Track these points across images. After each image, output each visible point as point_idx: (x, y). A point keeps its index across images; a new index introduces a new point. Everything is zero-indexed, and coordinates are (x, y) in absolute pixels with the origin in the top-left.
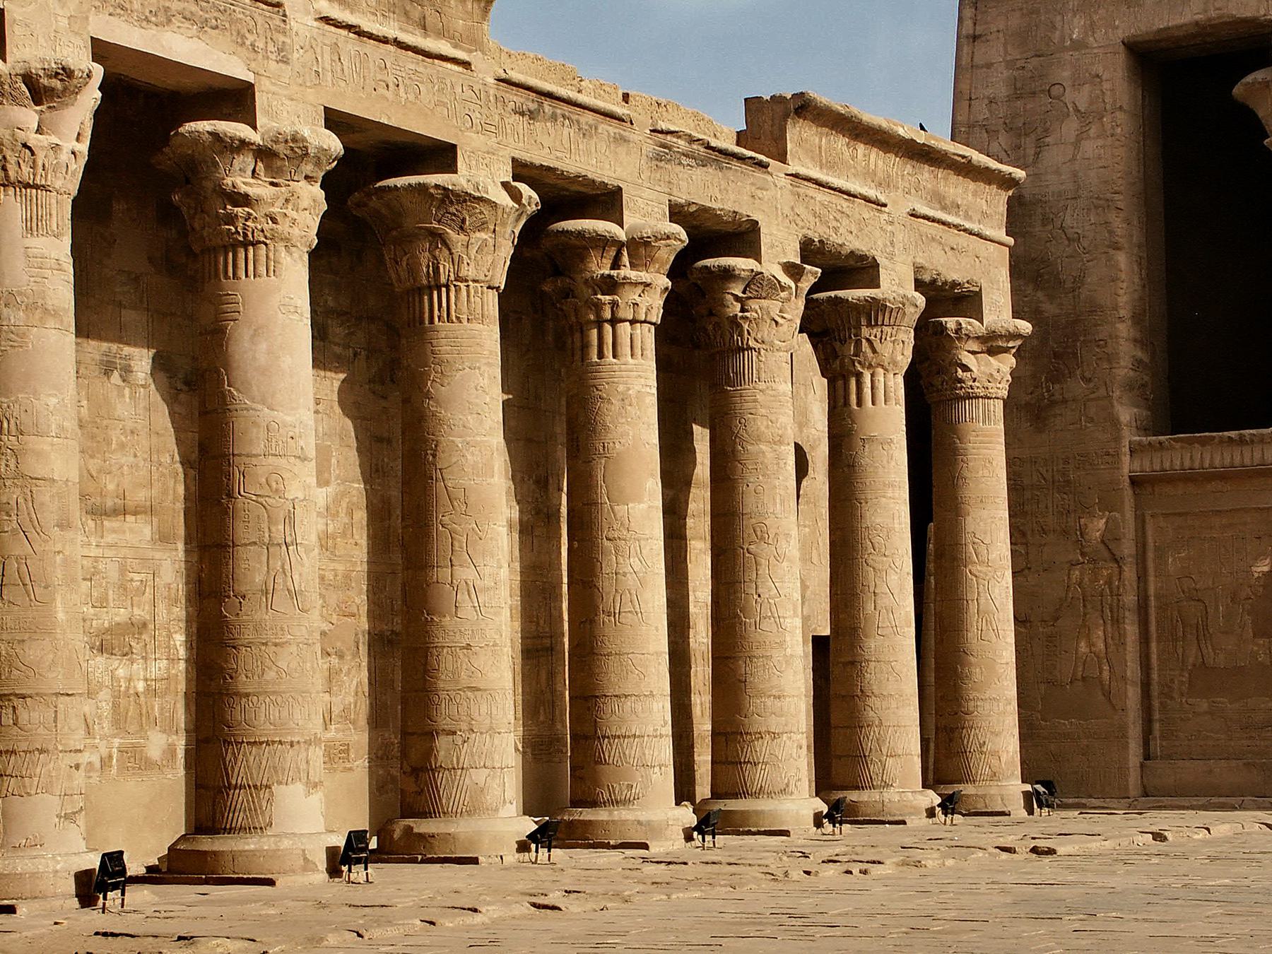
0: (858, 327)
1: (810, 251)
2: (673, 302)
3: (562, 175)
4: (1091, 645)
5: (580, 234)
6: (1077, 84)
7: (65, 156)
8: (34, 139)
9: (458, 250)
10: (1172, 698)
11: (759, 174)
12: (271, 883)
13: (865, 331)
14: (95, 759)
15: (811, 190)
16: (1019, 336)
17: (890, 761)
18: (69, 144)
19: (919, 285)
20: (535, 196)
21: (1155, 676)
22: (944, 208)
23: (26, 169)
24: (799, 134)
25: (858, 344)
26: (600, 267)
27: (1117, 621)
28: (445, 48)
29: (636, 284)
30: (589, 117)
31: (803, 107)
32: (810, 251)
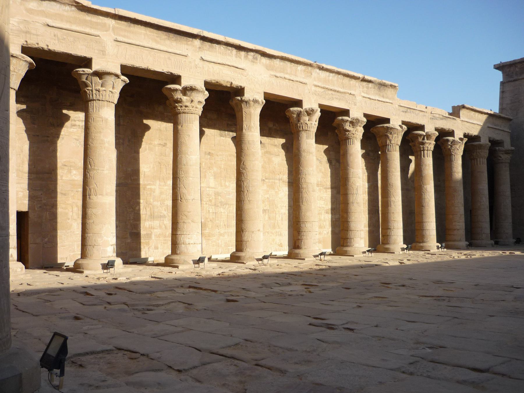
1: (465, 136)
2: (436, 146)
3: (412, 123)
5: (416, 134)
7: (313, 125)
8: (308, 122)
9: (391, 138)
11: (454, 121)
12: (353, 256)
14: (326, 232)
15: (466, 123)
18: (314, 123)
19: (490, 141)
20: (406, 127)
23: (306, 128)
24: (463, 112)
26: (420, 140)
28: (387, 100)
30: (417, 112)
31: (463, 107)
32: (465, 136)
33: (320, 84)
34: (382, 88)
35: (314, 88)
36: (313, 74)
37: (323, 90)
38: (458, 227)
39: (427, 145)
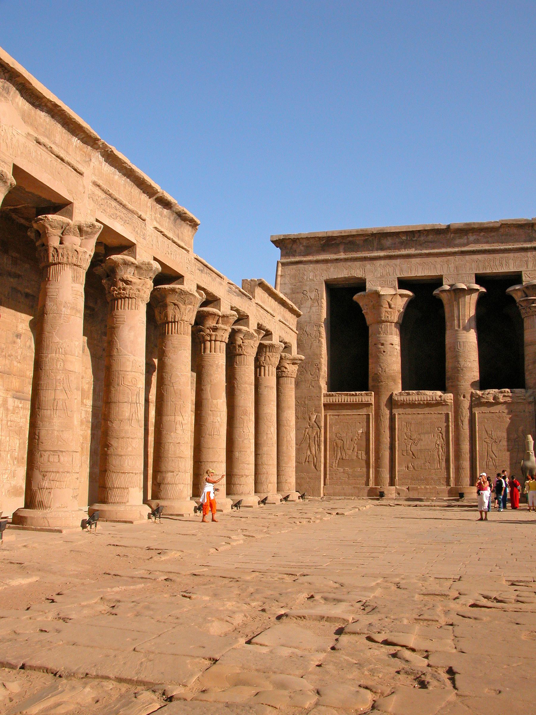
0: (265, 352)
4: (311, 451)
6: (311, 291)
8: (79, 249)
9: (182, 310)
10: (332, 467)
13: (268, 354)
15: (259, 308)
16: (301, 360)
17: (270, 485)
21: (328, 461)
22: (285, 320)
25: (265, 357)
27: (319, 446)
29: (223, 329)
30: (214, 275)
33: (100, 182)
34: (179, 221)
35: (91, 187)
36: (93, 160)
37: (104, 196)
38: (247, 472)
39: (219, 333)
